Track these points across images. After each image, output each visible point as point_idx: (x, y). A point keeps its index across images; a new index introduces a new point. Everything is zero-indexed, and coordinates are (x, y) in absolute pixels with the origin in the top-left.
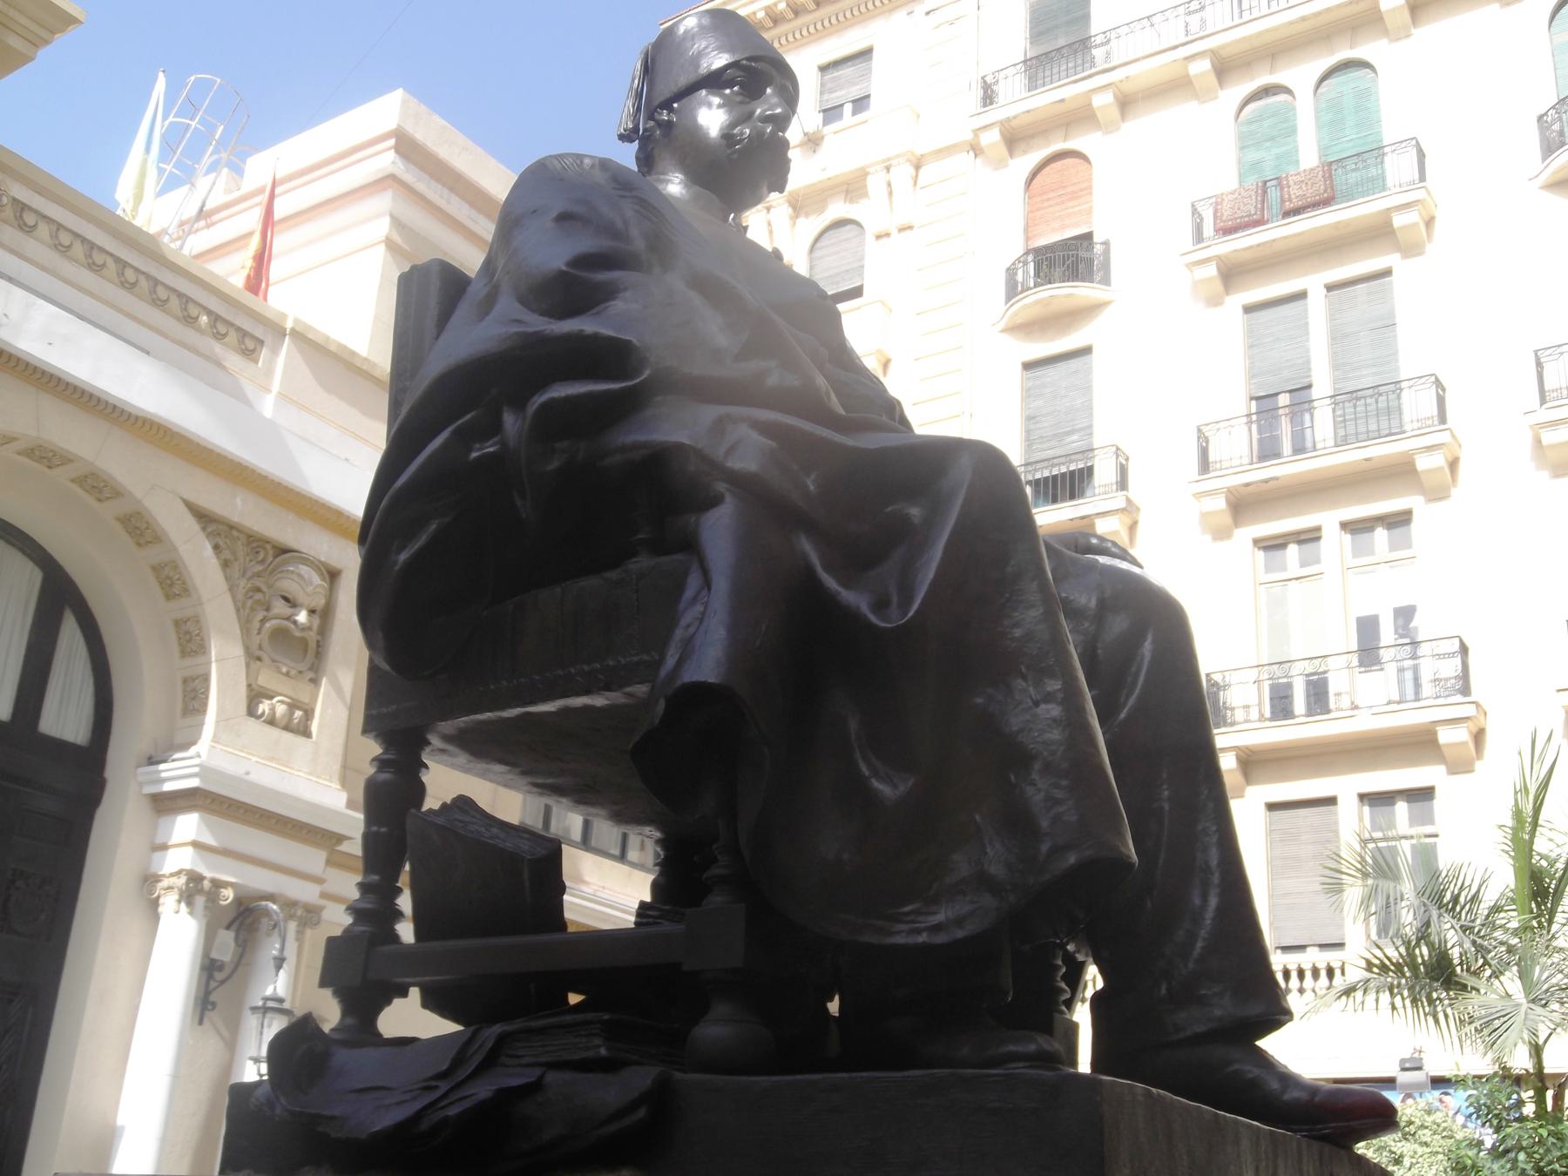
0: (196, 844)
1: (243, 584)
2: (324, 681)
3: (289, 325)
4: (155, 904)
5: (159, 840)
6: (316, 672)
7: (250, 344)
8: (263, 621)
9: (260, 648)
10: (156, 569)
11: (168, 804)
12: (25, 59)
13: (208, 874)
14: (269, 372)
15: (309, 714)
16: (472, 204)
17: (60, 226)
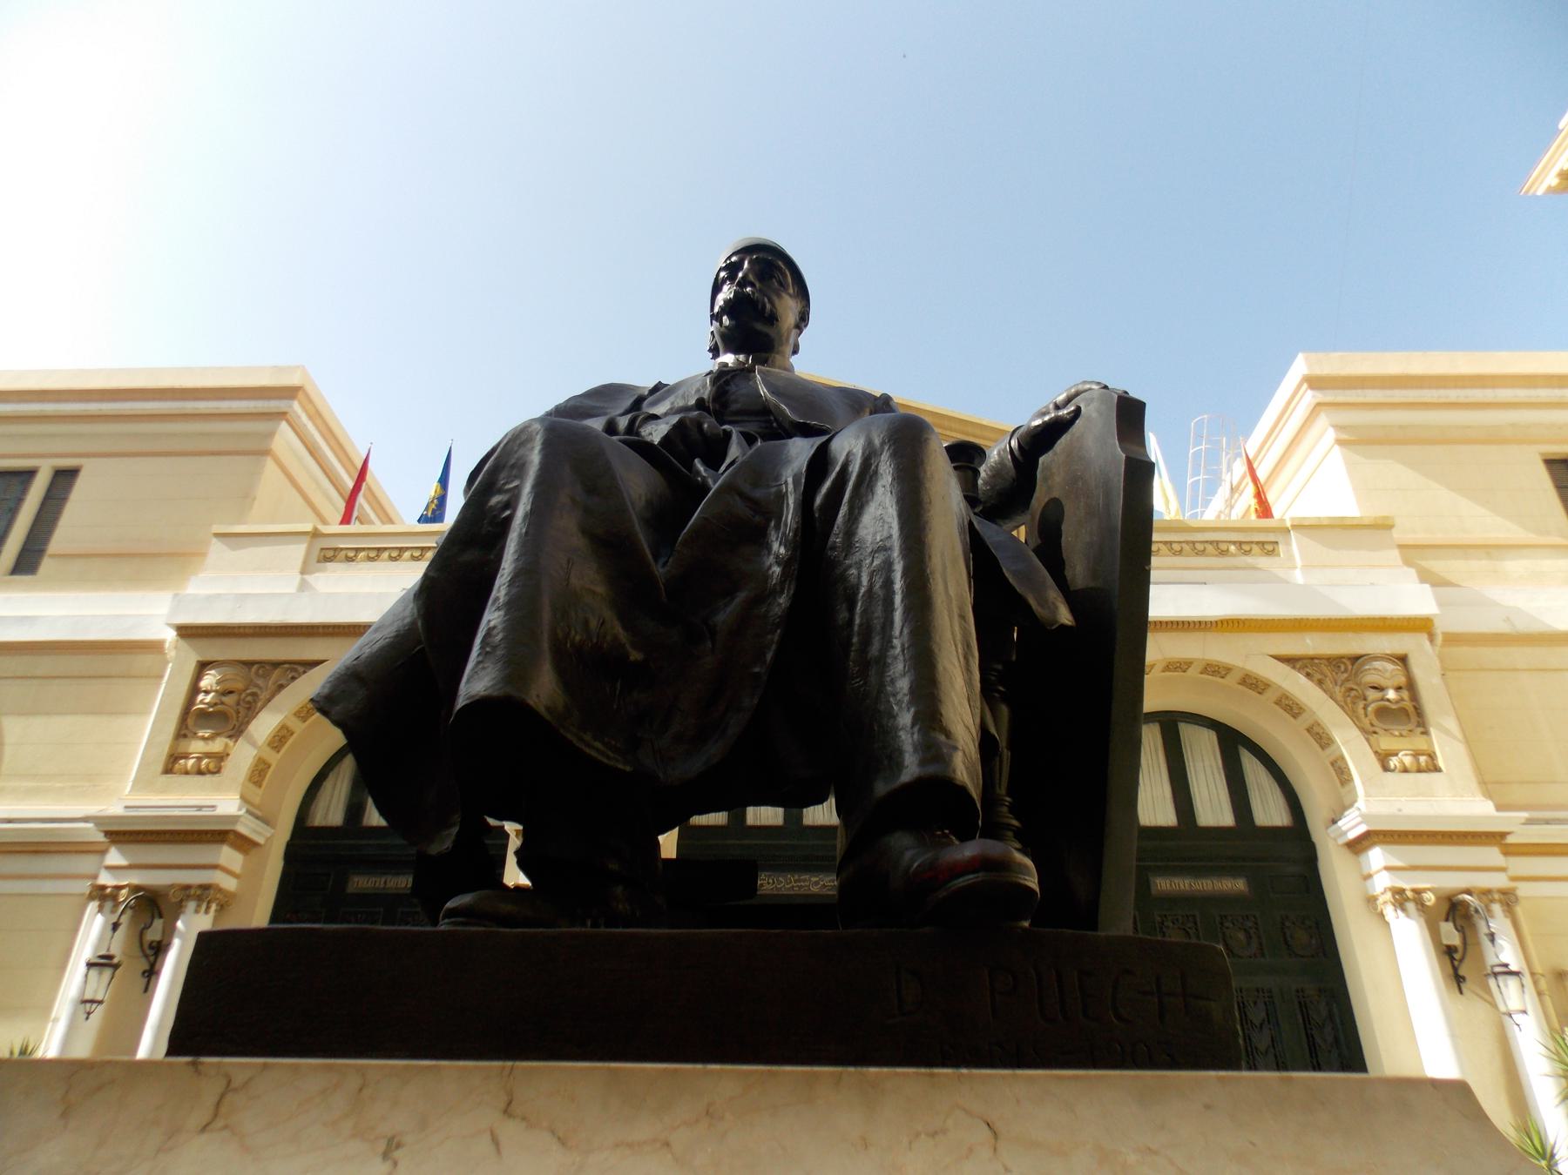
0: (1387, 868)
2: (1432, 731)
3: (1288, 524)
4: (1382, 915)
5: (1365, 872)
7: (1269, 547)
8: (1365, 708)
10: (1278, 703)
11: (1358, 846)
14: (1291, 558)
15: (1432, 756)
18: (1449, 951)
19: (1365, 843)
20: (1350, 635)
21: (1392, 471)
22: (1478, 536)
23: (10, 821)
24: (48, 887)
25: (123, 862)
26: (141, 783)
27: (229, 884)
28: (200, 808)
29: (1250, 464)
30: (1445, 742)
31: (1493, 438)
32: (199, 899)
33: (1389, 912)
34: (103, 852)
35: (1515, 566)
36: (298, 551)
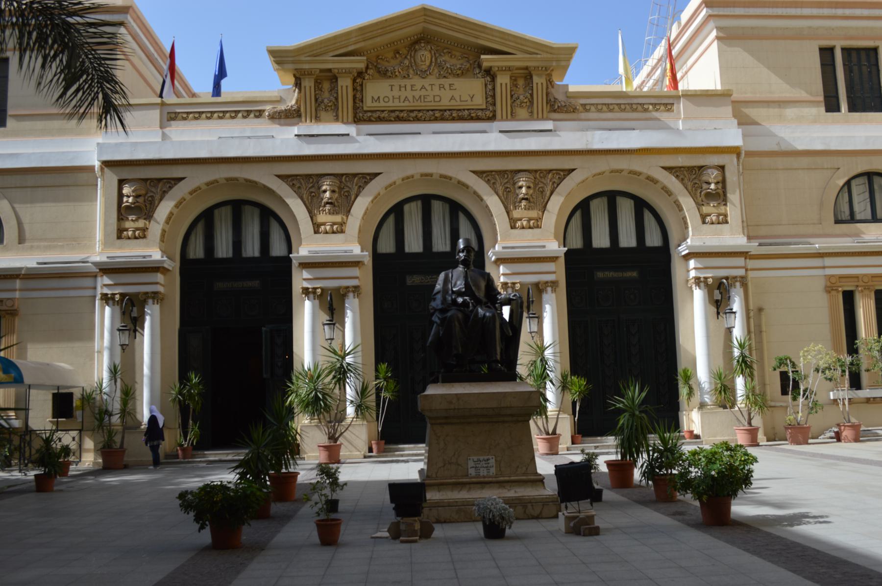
0: (695, 268)
1: (690, 185)
14: (679, 112)
15: (726, 216)
16: (744, 7)
18: (717, 301)
22: (776, 96)
23: (45, 263)
24: (72, 293)
25: (110, 282)
26: (106, 244)
27: (161, 289)
28: (144, 257)
30: (733, 210)
31: (798, 36)
32: (153, 298)
34: (96, 276)
35: (790, 112)
36: (156, 114)
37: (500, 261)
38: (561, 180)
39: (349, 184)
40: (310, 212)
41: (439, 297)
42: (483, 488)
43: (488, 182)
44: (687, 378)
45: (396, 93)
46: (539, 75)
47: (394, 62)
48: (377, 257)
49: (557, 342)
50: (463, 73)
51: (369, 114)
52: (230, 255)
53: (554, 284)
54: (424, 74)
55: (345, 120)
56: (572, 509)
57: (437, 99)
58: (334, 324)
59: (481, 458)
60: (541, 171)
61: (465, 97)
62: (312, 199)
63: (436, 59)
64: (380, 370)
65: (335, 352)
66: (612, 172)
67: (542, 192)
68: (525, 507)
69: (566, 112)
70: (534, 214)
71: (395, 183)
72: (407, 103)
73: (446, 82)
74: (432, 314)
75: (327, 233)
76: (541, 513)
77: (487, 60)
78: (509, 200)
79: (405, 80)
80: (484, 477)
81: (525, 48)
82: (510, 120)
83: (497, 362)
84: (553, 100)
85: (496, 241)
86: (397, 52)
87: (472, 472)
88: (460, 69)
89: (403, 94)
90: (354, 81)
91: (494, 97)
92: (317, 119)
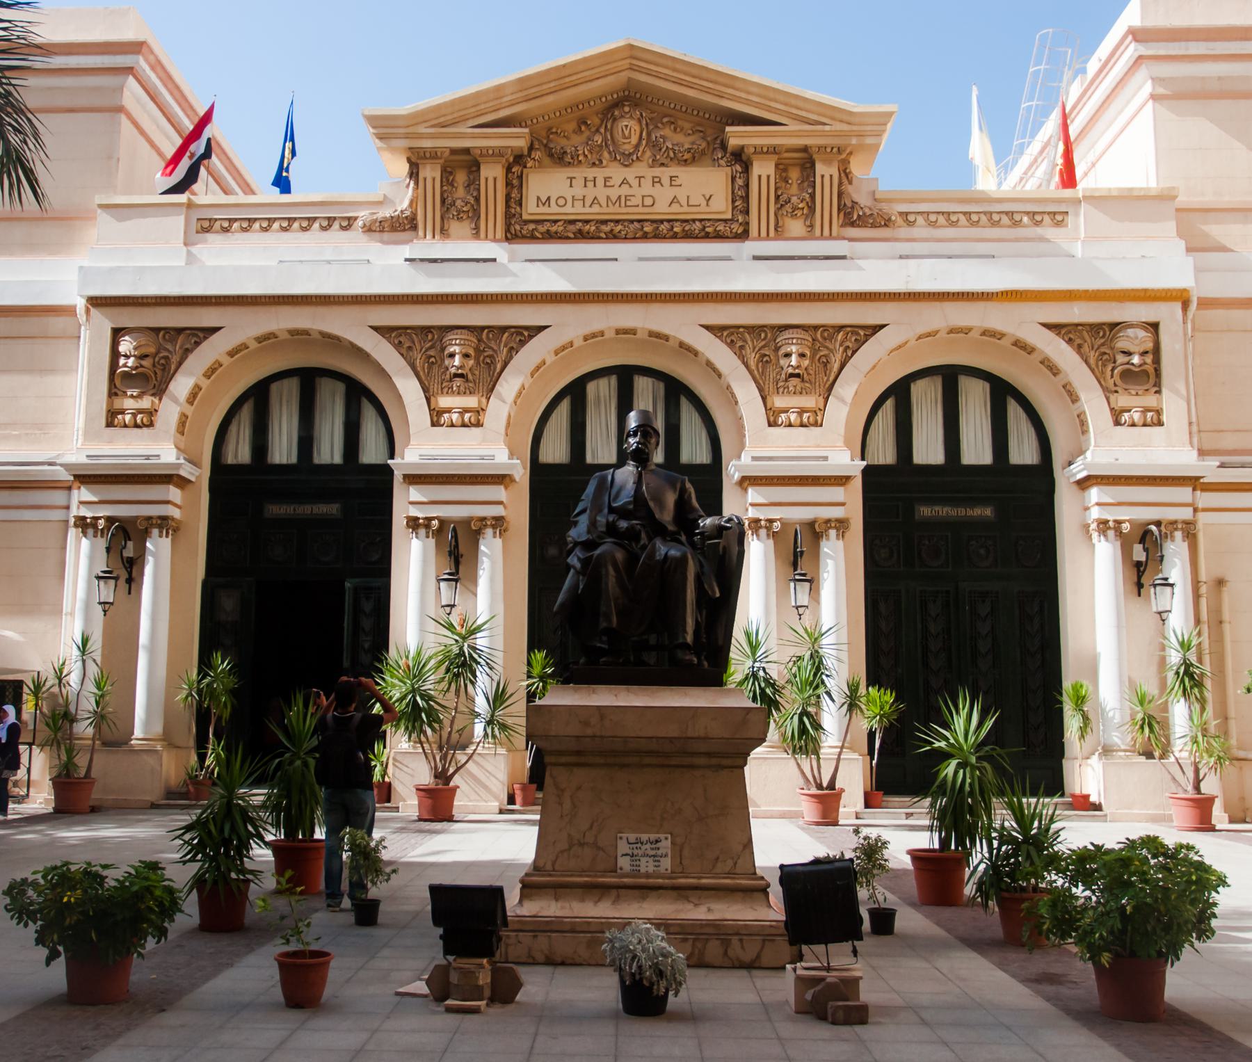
0: (1098, 504)
2: (1164, 390)
6: (1160, 386)
7: (1059, 218)
8: (1113, 370)
9: (1115, 385)
12: (877, 146)
13: (1110, 518)
14: (1077, 228)
17: (928, 213)
19: (1088, 483)
20: (1114, 304)
21: (1198, 128)
29: (1065, 117)
33: (1095, 535)
37: (747, 481)
38: (860, 343)
39: (493, 344)
40: (425, 390)
41: (584, 521)
42: (644, 898)
43: (731, 344)
44: (1080, 701)
45: (578, 191)
46: (828, 162)
47: (577, 140)
48: (538, 470)
49: (844, 621)
50: (692, 159)
51: (531, 226)
52: (294, 460)
53: (841, 525)
54: (627, 159)
55: (490, 235)
56: (815, 958)
57: (648, 201)
58: (456, 581)
59: (644, 837)
60: (825, 327)
61: (697, 199)
62: (430, 368)
63: (649, 135)
64: (534, 664)
65: (450, 627)
66: (951, 331)
67: (825, 364)
68: (726, 943)
69: (873, 226)
70: (809, 402)
71: (571, 344)
72: (596, 209)
73: (665, 173)
74: (570, 552)
75: (452, 425)
76: (758, 956)
77: (737, 136)
78: (768, 379)
79: (595, 169)
80: (648, 876)
81: (804, 114)
82: (775, 239)
83: (685, 646)
84: (849, 204)
85: (742, 446)
86: (583, 122)
87: (624, 863)
88: (689, 150)
89: (590, 192)
90: (509, 170)
91: (746, 198)
92: (444, 233)
